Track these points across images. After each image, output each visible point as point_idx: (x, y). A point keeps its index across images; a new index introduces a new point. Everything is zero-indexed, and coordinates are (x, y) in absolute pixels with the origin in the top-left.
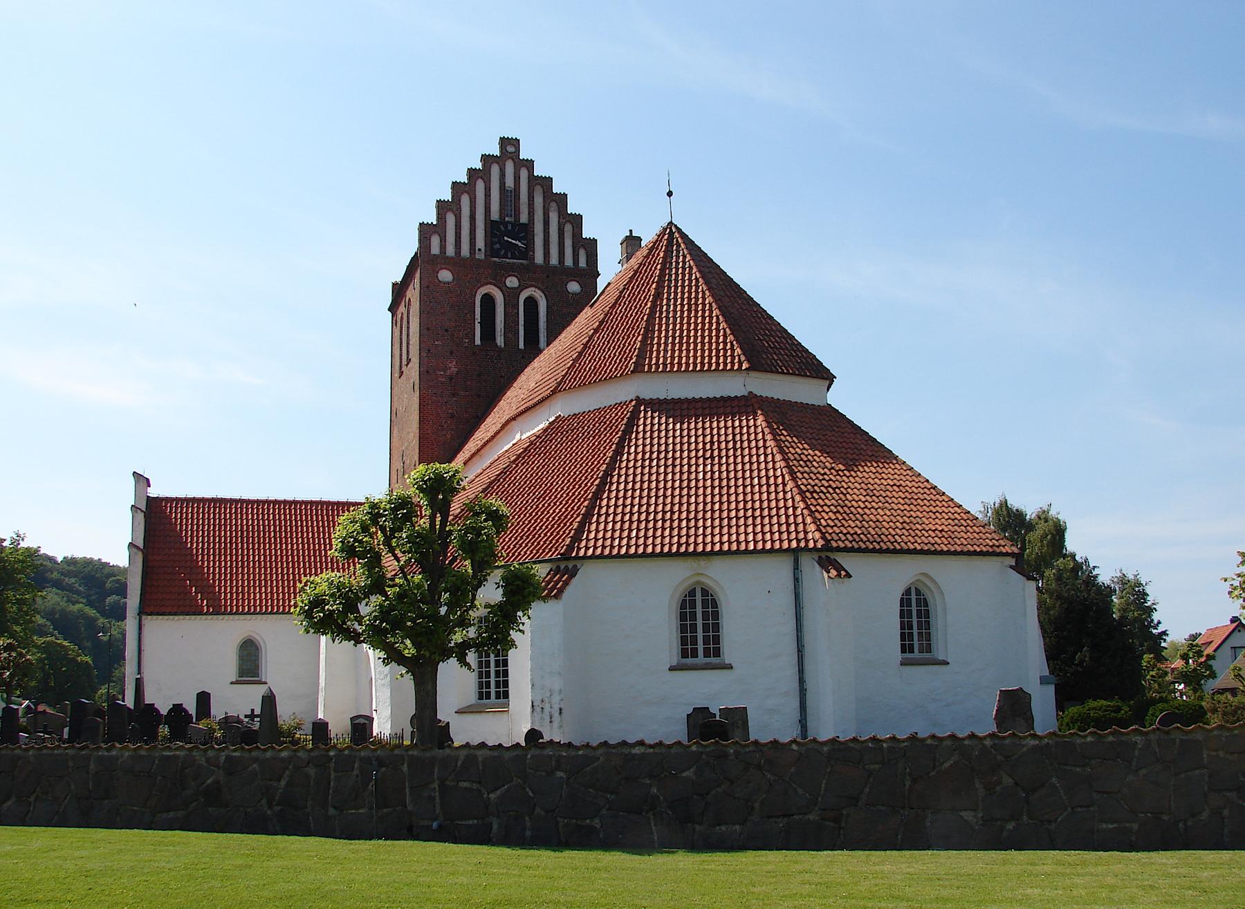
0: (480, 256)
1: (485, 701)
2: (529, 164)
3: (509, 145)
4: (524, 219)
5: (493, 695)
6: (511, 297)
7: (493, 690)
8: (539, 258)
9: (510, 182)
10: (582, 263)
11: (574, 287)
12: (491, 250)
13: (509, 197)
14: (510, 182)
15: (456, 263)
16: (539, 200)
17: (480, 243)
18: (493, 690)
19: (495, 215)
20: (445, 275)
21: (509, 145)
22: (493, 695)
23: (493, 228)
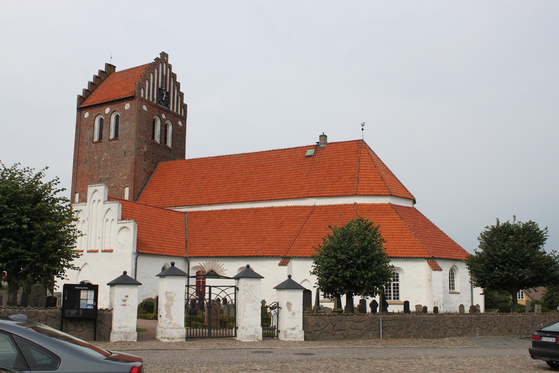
0: (155, 102)
1: (396, 300)
2: (170, 67)
3: (164, 55)
4: (168, 91)
5: (392, 298)
6: (162, 121)
7: (392, 297)
8: (171, 109)
9: (165, 73)
10: (183, 115)
11: (180, 123)
12: (159, 102)
13: (164, 78)
14: (165, 73)
15: (148, 103)
16: (172, 83)
17: (155, 97)
18: (392, 297)
19: (160, 86)
20: (145, 108)
21: (164, 55)
22: (392, 298)
23: (159, 90)
